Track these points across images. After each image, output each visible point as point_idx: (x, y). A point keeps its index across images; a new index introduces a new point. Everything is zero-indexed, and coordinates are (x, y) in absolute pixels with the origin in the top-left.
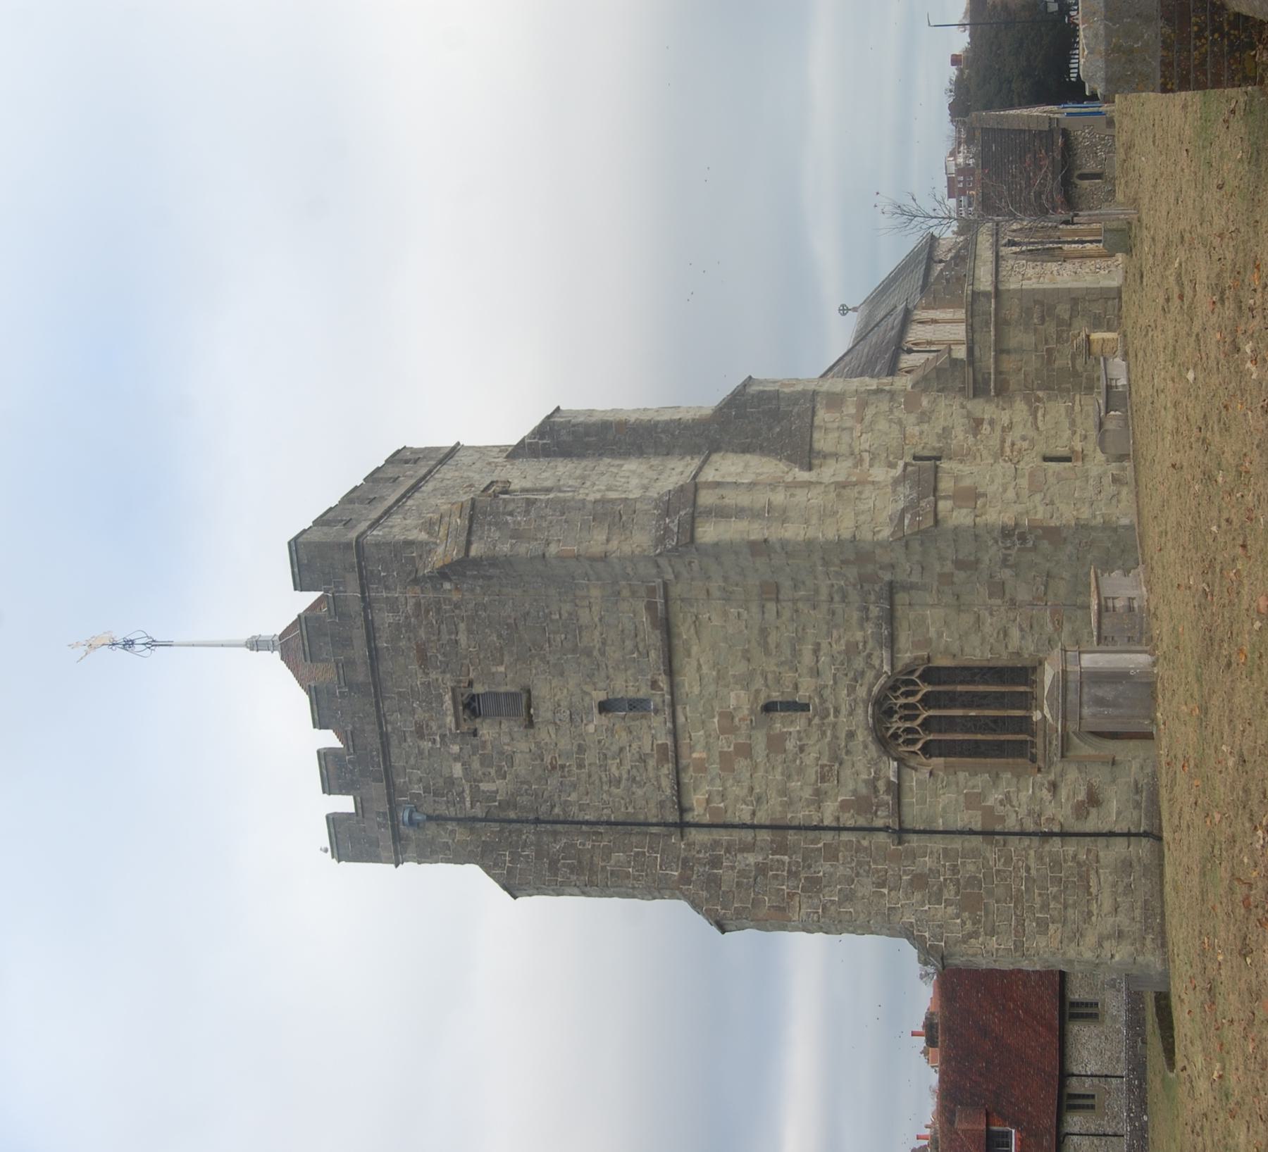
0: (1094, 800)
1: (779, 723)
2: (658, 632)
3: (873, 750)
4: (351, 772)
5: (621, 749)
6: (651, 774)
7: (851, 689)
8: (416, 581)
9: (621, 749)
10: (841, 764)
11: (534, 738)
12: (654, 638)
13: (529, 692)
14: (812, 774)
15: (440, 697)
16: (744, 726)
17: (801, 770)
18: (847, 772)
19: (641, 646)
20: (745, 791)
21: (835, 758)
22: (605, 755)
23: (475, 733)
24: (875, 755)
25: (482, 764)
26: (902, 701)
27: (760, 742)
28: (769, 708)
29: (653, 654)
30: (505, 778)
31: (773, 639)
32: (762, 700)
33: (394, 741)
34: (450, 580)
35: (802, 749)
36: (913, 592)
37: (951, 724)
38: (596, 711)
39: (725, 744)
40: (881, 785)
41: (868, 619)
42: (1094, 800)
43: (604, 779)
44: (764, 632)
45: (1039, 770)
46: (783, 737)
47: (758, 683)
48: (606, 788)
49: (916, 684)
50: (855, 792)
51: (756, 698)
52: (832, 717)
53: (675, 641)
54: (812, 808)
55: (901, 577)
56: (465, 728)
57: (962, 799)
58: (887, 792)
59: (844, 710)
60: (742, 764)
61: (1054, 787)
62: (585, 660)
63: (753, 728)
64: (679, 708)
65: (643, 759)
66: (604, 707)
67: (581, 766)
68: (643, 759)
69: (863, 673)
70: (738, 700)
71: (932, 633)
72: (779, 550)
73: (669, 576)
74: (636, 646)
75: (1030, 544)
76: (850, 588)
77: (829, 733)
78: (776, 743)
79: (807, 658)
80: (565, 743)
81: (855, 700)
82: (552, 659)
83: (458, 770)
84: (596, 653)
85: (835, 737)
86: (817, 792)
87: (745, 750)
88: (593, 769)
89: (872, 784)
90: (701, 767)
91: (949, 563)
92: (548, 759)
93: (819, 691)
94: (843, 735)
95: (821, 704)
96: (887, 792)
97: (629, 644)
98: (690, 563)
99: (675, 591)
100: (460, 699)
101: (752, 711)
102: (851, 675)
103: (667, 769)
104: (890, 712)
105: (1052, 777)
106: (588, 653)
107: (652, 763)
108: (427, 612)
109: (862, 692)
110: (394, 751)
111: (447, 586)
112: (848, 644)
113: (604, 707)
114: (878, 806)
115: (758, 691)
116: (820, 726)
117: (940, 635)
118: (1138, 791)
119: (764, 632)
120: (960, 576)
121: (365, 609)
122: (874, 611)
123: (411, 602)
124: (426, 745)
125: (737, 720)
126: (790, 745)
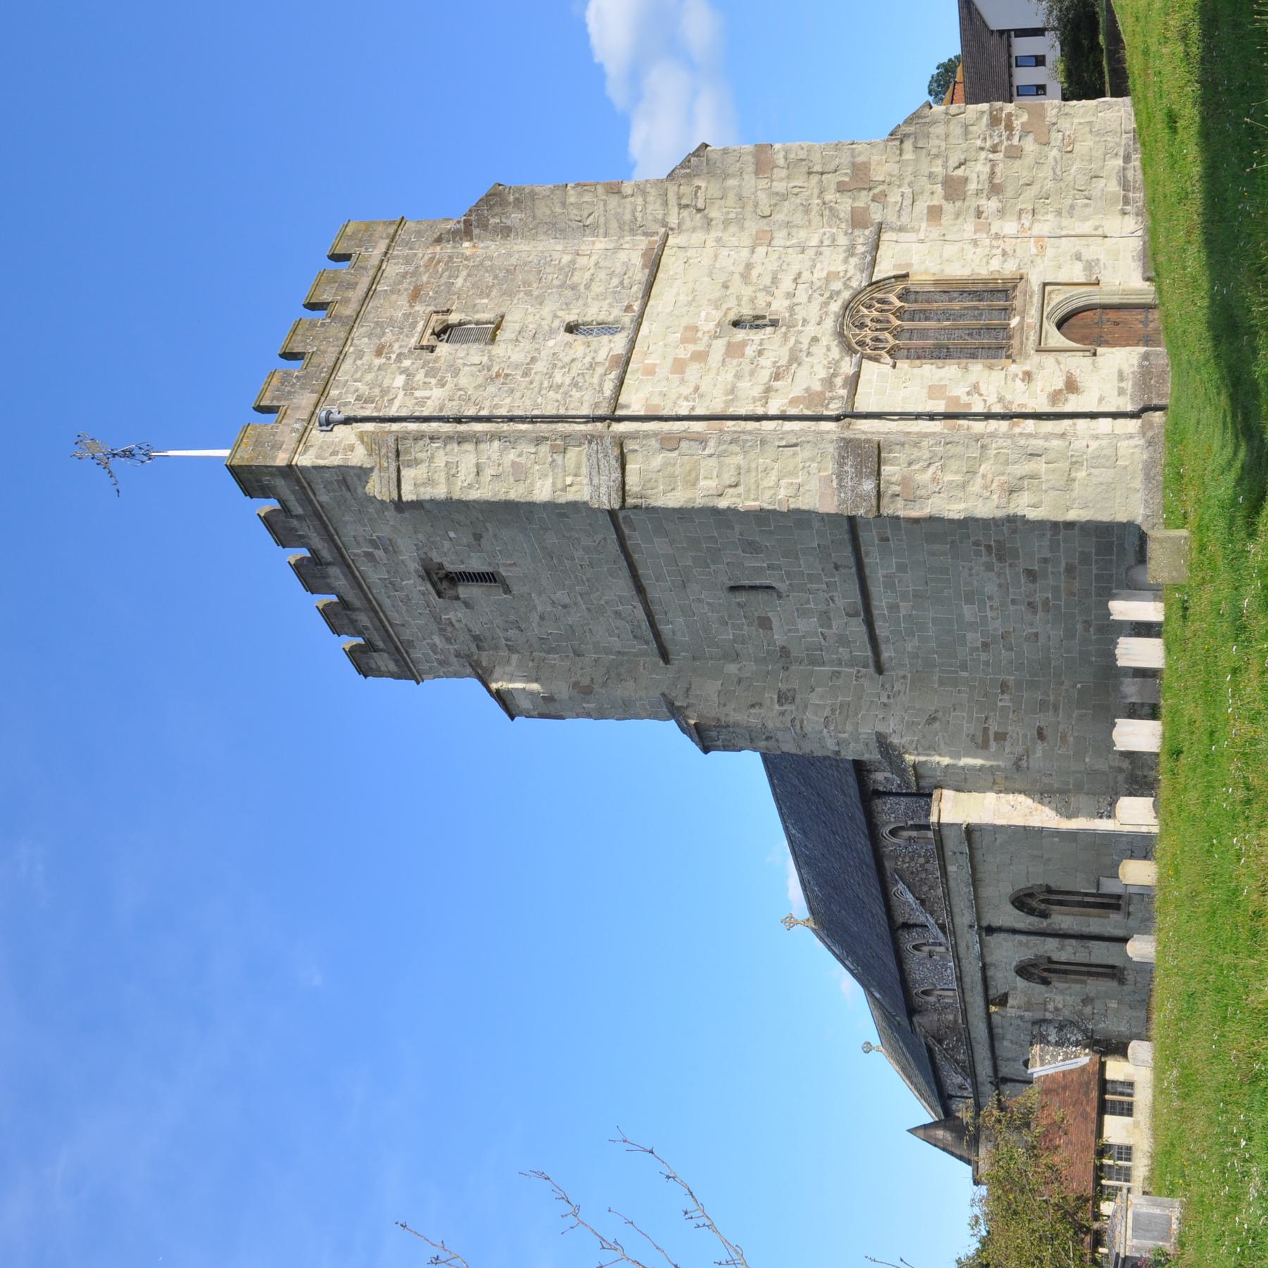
0: (1072, 386)
1: (740, 335)
2: (647, 271)
3: (836, 352)
4: (294, 384)
5: (573, 360)
6: (596, 380)
7: (826, 304)
8: (439, 240)
9: (573, 360)
10: (799, 364)
11: (489, 351)
12: (641, 275)
13: (503, 317)
14: (764, 375)
15: (414, 325)
16: (706, 338)
17: (752, 373)
18: (803, 372)
19: (626, 282)
20: (691, 390)
21: (794, 358)
22: (555, 365)
23: (432, 349)
24: (837, 357)
25: (426, 376)
26: (875, 314)
27: (720, 345)
28: (736, 324)
29: (635, 288)
30: (443, 386)
31: (754, 273)
32: (732, 316)
33: (349, 361)
34: (471, 240)
35: (760, 353)
36: (902, 234)
37: (923, 334)
38: (562, 329)
39: (684, 353)
40: (839, 381)
41: (852, 255)
42: (1072, 386)
43: (546, 384)
44: (749, 266)
45: (1014, 361)
46: (744, 344)
47: (732, 303)
48: (543, 392)
49: (890, 303)
50: (807, 390)
51: (726, 314)
52: (799, 328)
53: (660, 275)
54: (758, 403)
55: (891, 217)
56: (424, 343)
57: (926, 390)
58: (844, 386)
59: (813, 322)
60: (693, 370)
61: (1028, 376)
62: (569, 293)
63: (716, 338)
64: (644, 323)
65: (592, 367)
66: (571, 329)
67: (525, 374)
68: (592, 367)
69: (838, 293)
70: (707, 319)
71: (915, 260)
72: (781, 162)
73: (673, 220)
74: (622, 283)
75: (1015, 141)
76: (841, 234)
77: (792, 341)
78: (734, 350)
79: (786, 284)
80: (518, 356)
81: (826, 313)
82: (536, 293)
83: (400, 380)
84: (582, 288)
85: (797, 342)
86: (768, 390)
87: (700, 357)
88: (537, 378)
89: (829, 382)
90: (650, 371)
91: (939, 188)
92: (495, 369)
93: (791, 309)
94: (805, 342)
95: (791, 316)
96: (844, 386)
97: (615, 281)
98: (699, 188)
99: (671, 241)
100: (432, 324)
101: (719, 325)
102: (827, 295)
103: (613, 375)
104: (862, 326)
105: (1027, 368)
106: (574, 287)
107: (600, 370)
108: (439, 262)
109: (835, 307)
110: (346, 366)
111: (466, 244)
112: (828, 274)
113: (571, 329)
114: (832, 399)
115: (729, 309)
116: (785, 334)
117: (923, 262)
118: (1121, 377)
119: (749, 266)
120: (949, 207)
121: (382, 261)
122: (860, 249)
123: (426, 258)
124: (378, 362)
125: (700, 334)
126: (750, 351)
